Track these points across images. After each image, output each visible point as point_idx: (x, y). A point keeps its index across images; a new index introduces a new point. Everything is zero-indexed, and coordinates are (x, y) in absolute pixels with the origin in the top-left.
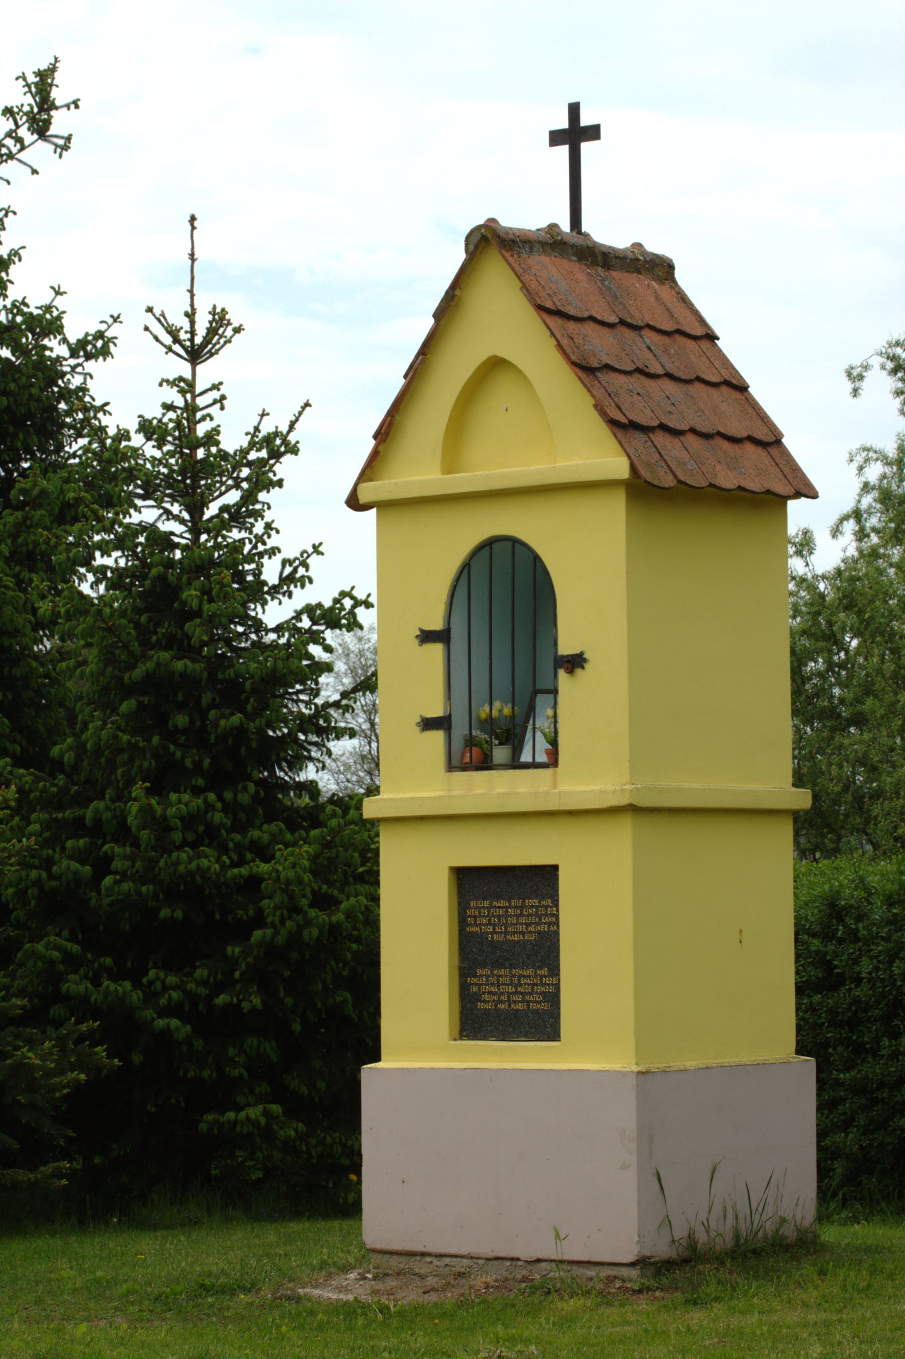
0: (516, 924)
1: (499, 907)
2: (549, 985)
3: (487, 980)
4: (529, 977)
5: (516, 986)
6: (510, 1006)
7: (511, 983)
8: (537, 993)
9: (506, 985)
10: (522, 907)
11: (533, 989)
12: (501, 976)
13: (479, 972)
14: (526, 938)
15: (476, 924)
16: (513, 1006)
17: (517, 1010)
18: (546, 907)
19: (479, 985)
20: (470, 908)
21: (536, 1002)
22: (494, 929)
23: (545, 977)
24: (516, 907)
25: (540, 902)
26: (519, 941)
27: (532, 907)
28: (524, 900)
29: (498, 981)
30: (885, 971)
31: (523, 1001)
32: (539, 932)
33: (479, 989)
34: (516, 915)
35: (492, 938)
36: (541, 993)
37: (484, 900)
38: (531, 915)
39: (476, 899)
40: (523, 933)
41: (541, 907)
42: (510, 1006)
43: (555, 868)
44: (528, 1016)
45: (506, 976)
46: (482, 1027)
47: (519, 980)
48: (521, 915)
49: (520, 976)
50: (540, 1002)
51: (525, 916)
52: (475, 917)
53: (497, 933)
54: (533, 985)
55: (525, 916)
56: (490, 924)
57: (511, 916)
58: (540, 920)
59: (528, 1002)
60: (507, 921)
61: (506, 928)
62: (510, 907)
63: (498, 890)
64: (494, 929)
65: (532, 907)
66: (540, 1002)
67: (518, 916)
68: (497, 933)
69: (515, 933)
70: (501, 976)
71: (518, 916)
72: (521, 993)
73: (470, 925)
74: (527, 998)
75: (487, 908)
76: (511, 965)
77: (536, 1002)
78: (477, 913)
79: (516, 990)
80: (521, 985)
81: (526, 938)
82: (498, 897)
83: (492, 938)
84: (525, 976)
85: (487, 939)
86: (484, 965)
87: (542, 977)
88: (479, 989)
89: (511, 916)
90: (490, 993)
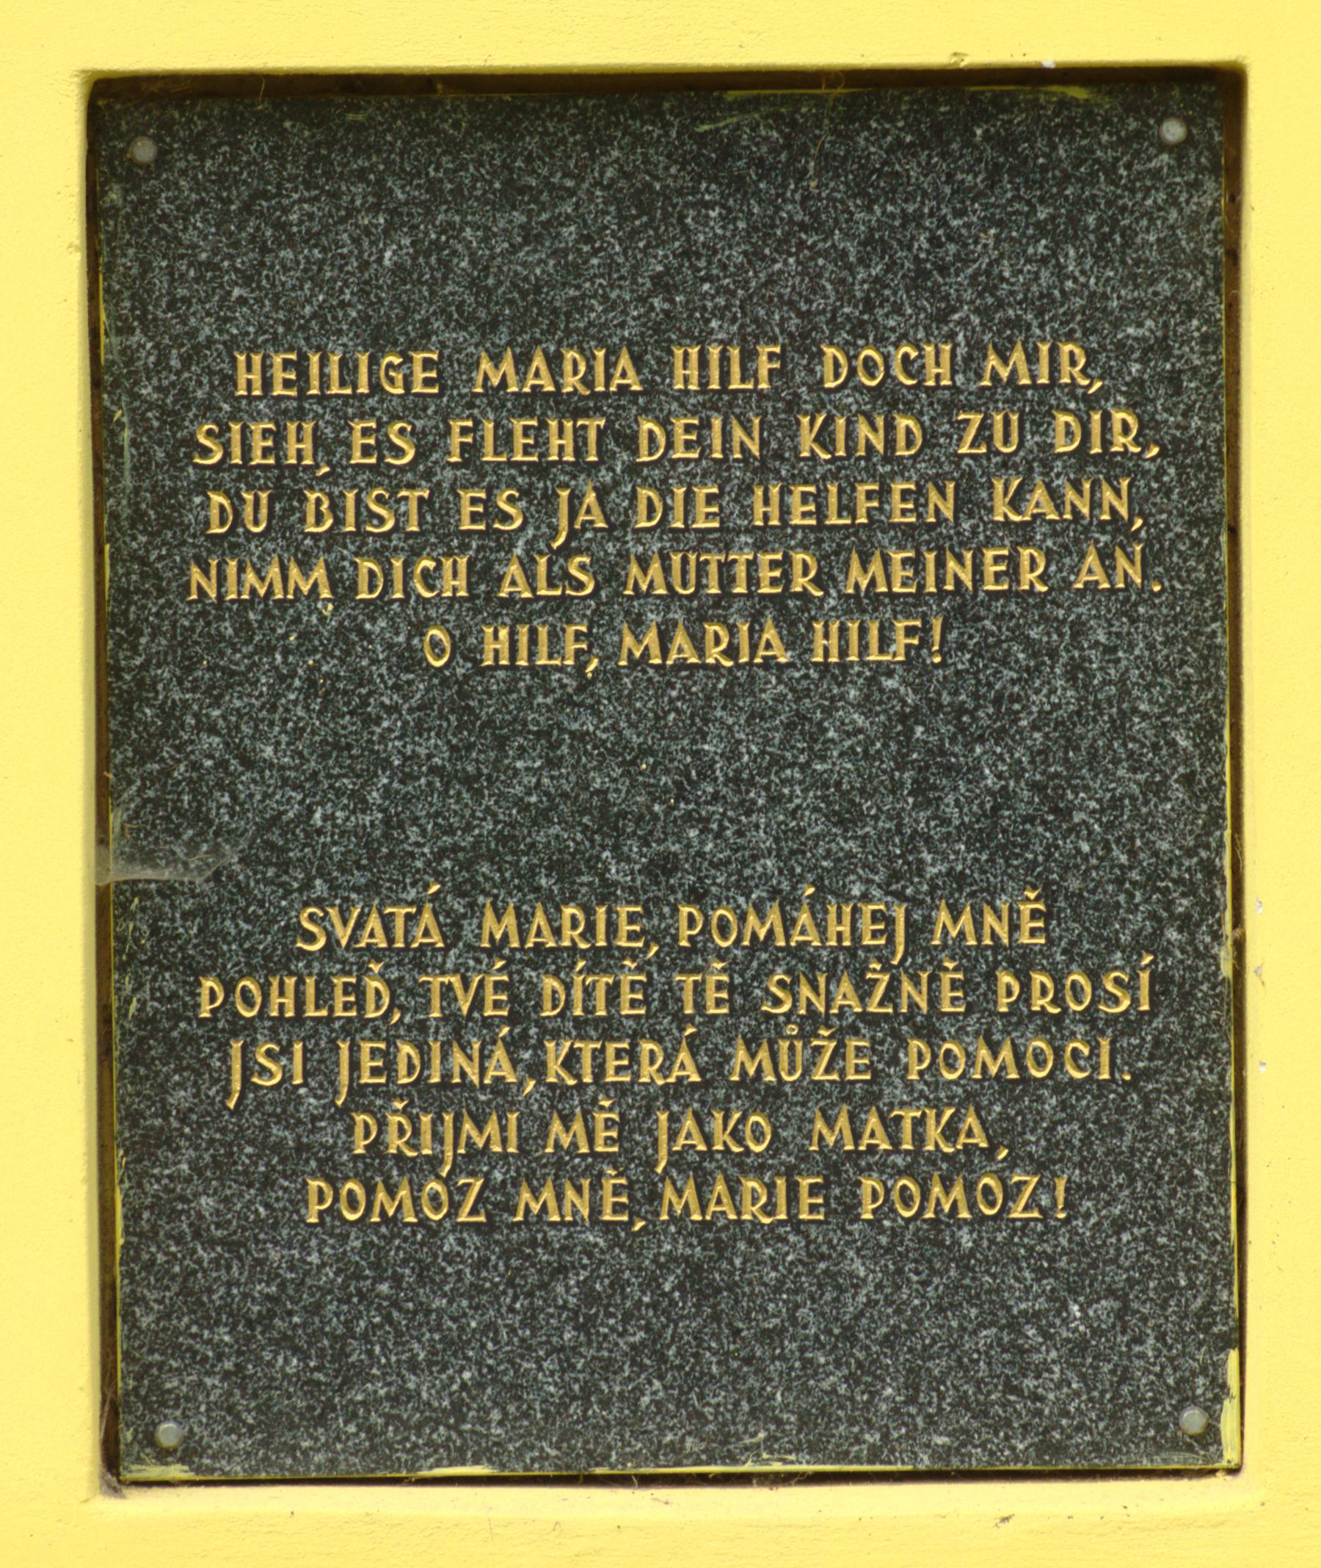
0: (724, 538)
1: (530, 403)
2: (1053, 1026)
3: (406, 993)
4: (851, 961)
5: (709, 1043)
6: (644, 1195)
7: (663, 1016)
8: (931, 1092)
9: (608, 1028)
10: (783, 405)
11: (886, 1063)
12: (559, 960)
13: (321, 926)
14: (824, 645)
15: (284, 536)
16: (678, 1199)
17: (720, 1238)
18: (1036, 406)
19: (321, 1039)
20: (226, 406)
21: (920, 1165)
22: (484, 574)
23: (1022, 963)
24: (720, 401)
25: (970, 363)
26: (738, 684)
27: (888, 399)
28: (803, 346)
29: (522, 1005)
30: (1040, 1099)
31: (785, 1162)
32: (962, 607)
33: (319, 1069)
34: (720, 470)
35: (466, 649)
36: (970, 1096)
37: (378, 341)
38: (884, 465)
39: (298, 331)
40: (792, 614)
41: (983, 400)
42: (644, 1195)
43: (1213, 95)
44: (840, 1283)
45: (603, 959)
46: (352, 1376)
47: (742, 993)
48: (773, 463)
49: (752, 963)
50: (962, 1166)
51: (806, 471)
52: (286, 485)
53: (519, 611)
54: (891, 1030)
55: (806, 471)
56: (438, 532)
57: (664, 475)
58: (970, 502)
59: (838, 1171)
60: (728, 512)
61: (609, 575)
62: (655, 397)
63: (537, 263)
64: (484, 574)
65: (888, 399)
66: (962, 1166)
67: (735, 477)
68: (519, 611)
69: (700, 613)
70: (559, 960)
71: (735, 477)
72: (768, 1097)
73: (232, 543)
74: (833, 1133)
75: (412, 406)
76: (662, 867)
77: (920, 1165)
78: (299, 447)
79: (714, 1068)
80: (762, 1032)
81: (824, 645)
82: (535, 319)
83: (466, 649)
84: (804, 962)
85: (410, 660)
86: (375, 869)
87: (979, 967)
88: (319, 1069)
89: (664, 475)
90: (434, 1096)
